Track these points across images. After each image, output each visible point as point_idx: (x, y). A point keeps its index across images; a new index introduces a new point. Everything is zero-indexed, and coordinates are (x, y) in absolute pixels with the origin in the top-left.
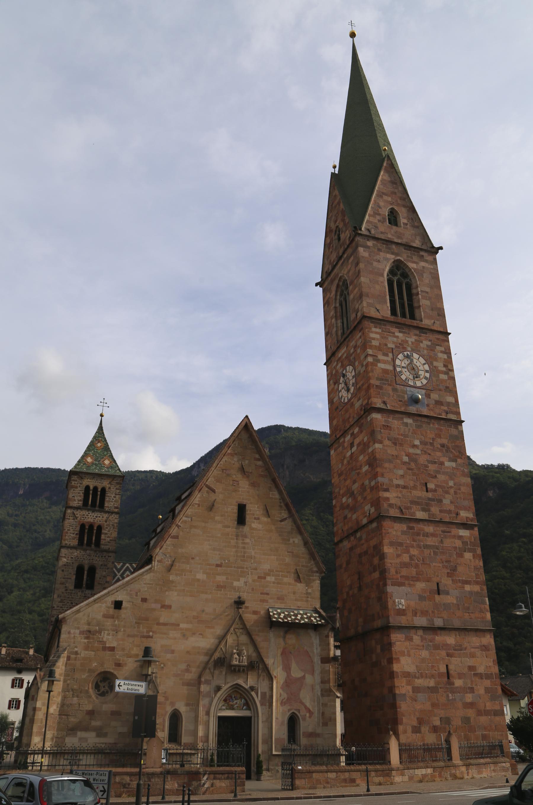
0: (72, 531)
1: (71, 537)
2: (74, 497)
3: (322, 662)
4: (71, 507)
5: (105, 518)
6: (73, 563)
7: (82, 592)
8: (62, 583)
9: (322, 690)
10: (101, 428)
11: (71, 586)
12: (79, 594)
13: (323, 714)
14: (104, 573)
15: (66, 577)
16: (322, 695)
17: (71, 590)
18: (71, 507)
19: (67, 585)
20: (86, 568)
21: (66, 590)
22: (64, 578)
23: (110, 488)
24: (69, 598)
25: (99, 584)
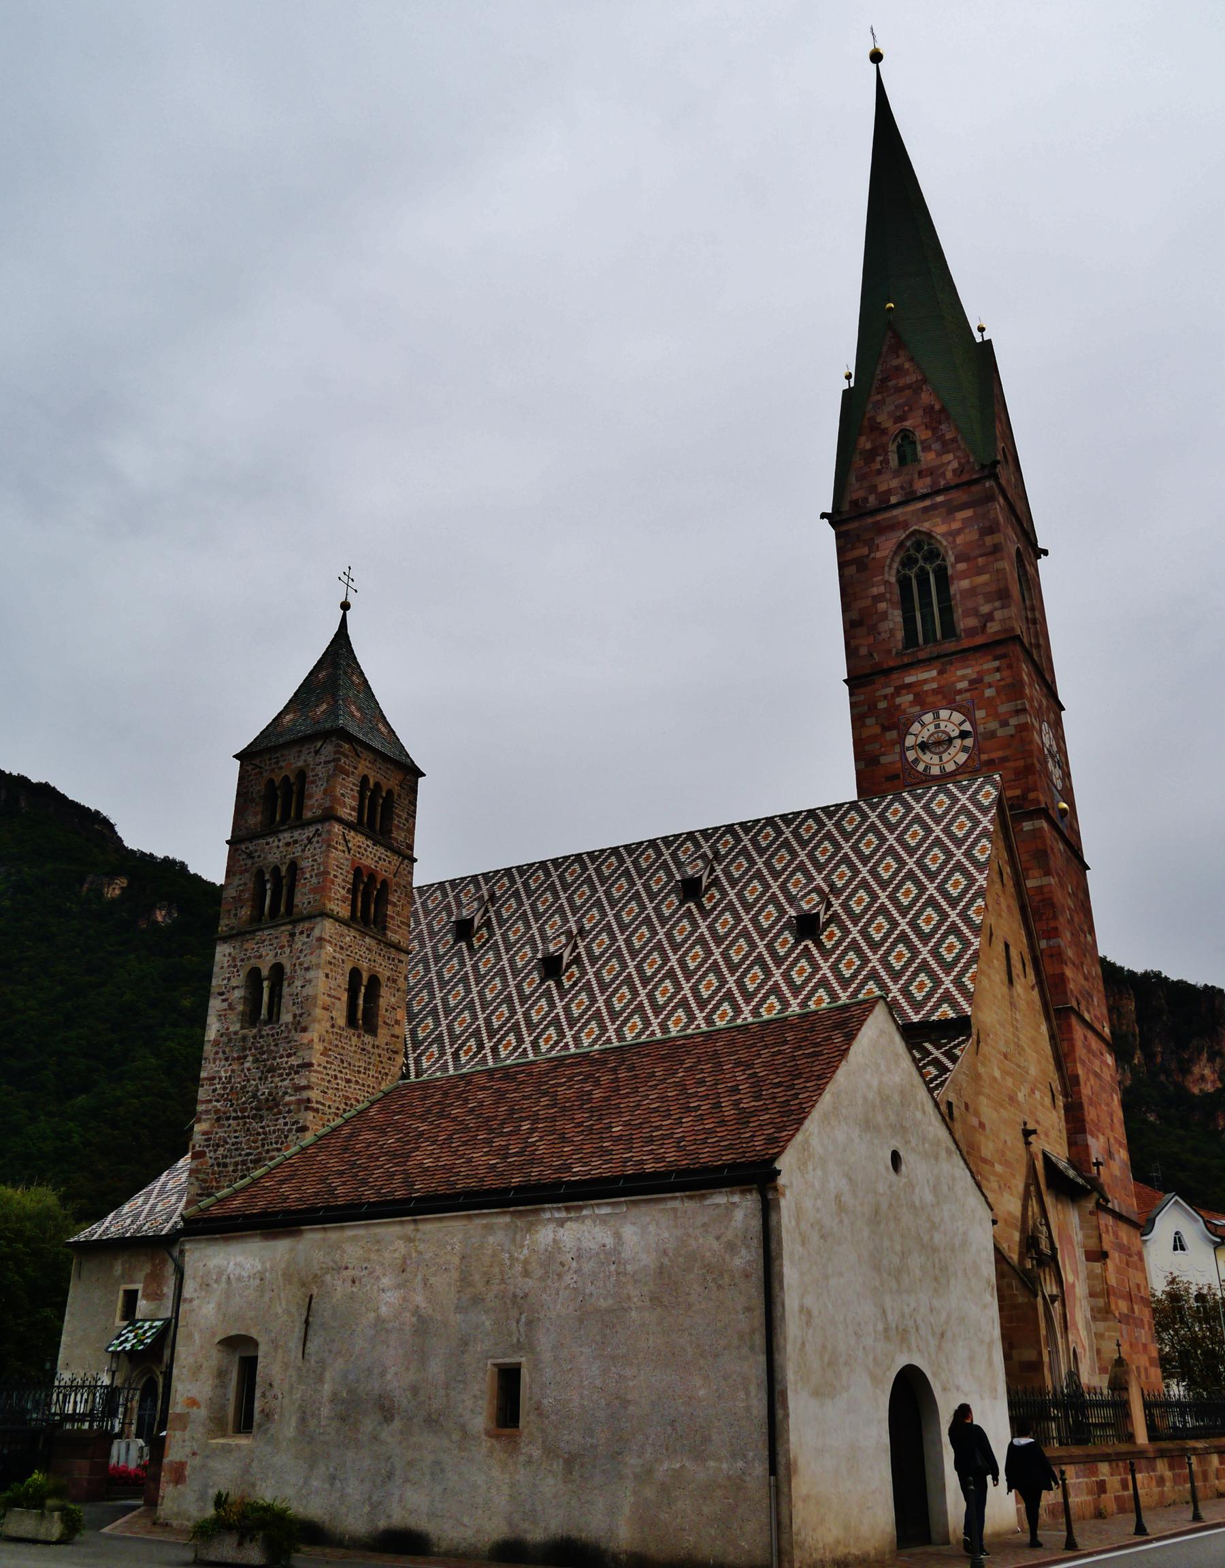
0: (339, 880)
1: (338, 896)
2: (343, 795)
3: (1088, 1259)
4: (340, 820)
5: (393, 868)
6: (343, 961)
7: (359, 1036)
8: (326, 1009)
9: (1092, 1310)
10: (341, 639)
11: (342, 1022)
12: (355, 1039)
13: (1098, 1351)
14: (393, 1000)
15: (333, 993)
16: (1094, 1318)
17: (340, 1028)
18: (340, 820)
19: (334, 1014)
20: (365, 976)
21: (333, 1026)
22: (329, 995)
23: (399, 796)
24: (337, 1046)
25: (385, 1023)
